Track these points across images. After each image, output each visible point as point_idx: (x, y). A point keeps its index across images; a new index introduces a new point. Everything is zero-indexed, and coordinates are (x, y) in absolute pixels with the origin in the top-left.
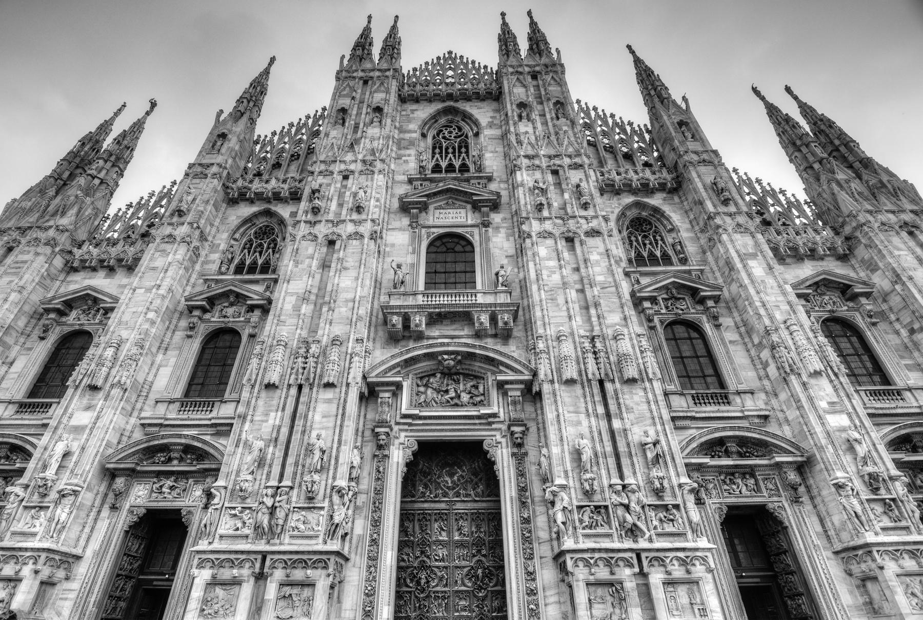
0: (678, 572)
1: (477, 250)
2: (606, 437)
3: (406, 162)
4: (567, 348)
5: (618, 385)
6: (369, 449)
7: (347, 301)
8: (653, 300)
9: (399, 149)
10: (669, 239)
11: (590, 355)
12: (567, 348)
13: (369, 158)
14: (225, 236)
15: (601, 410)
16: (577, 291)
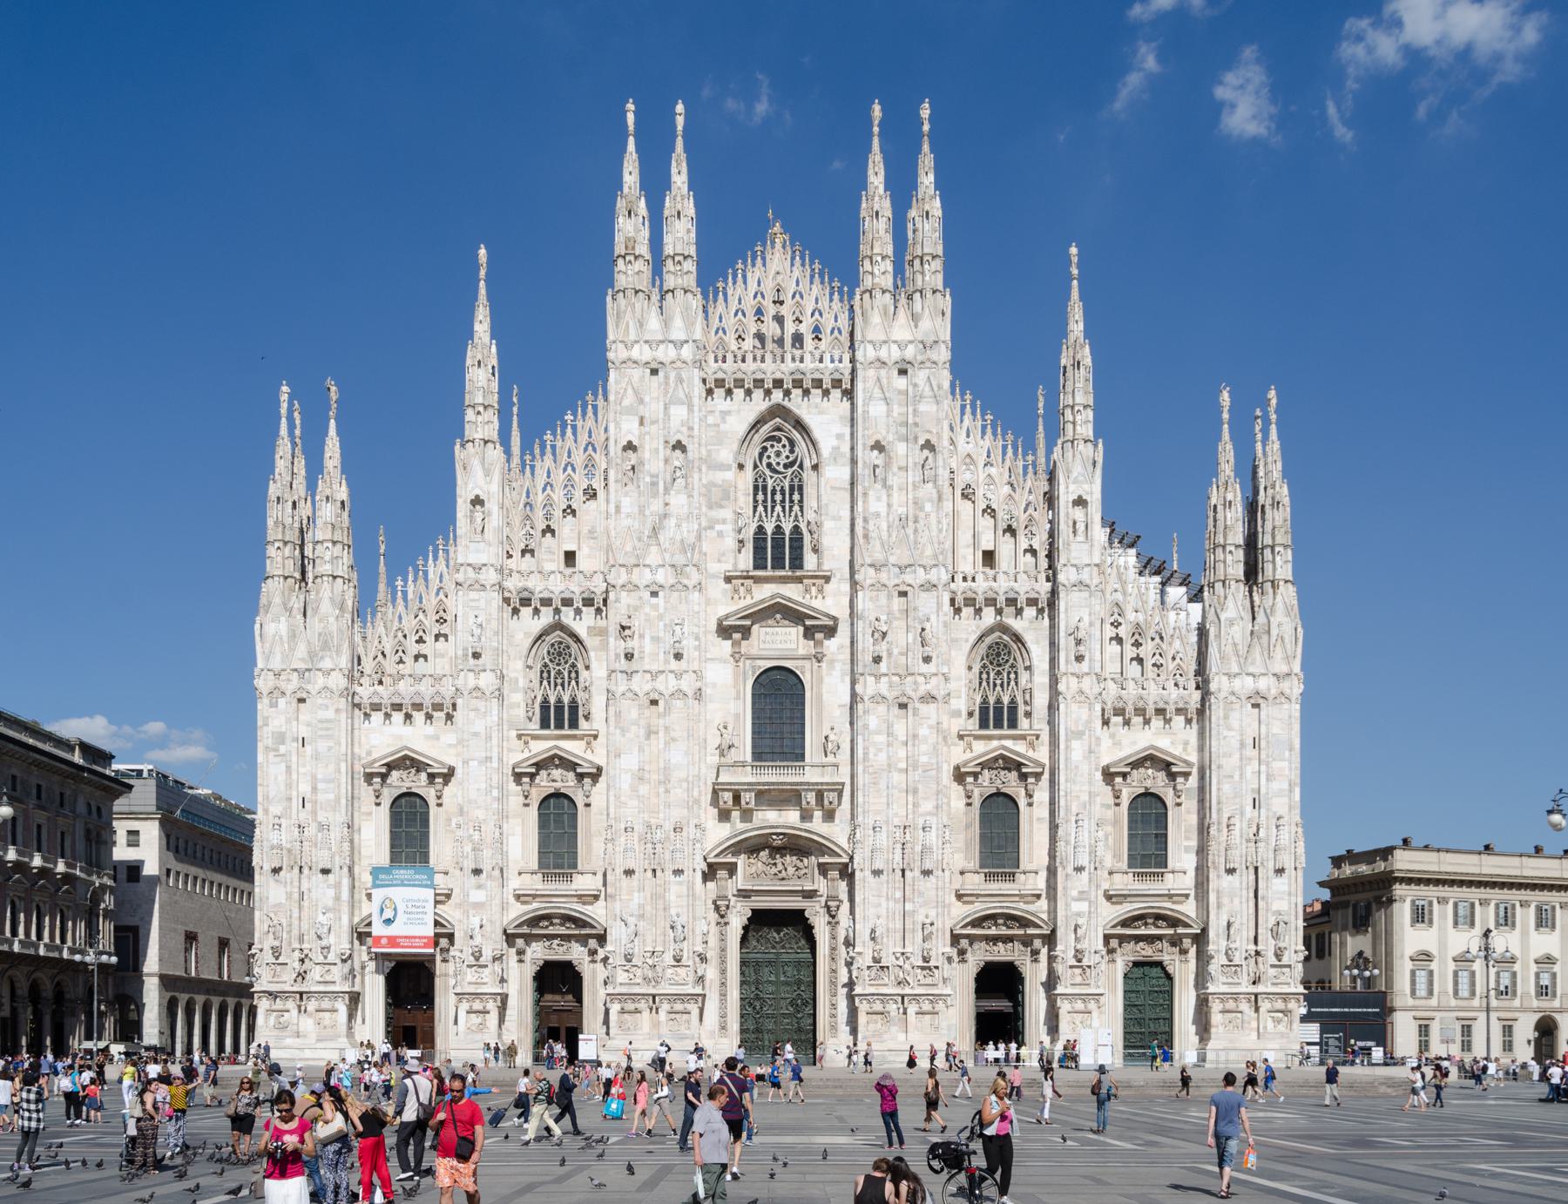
0: (927, 1007)
1: (808, 695)
2: (899, 917)
3: (720, 534)
4: (883, 839)
5: (917, 873)
6: (713, 916)
7: (680, 781)
8: (976, 775)
9: (710, 507)
10: (1024, 677)
11: (899, 846)
12: (883, 839)
13: (680, 559)
14: (519, 665)
15: (899, 894)
16: (900, 770)
